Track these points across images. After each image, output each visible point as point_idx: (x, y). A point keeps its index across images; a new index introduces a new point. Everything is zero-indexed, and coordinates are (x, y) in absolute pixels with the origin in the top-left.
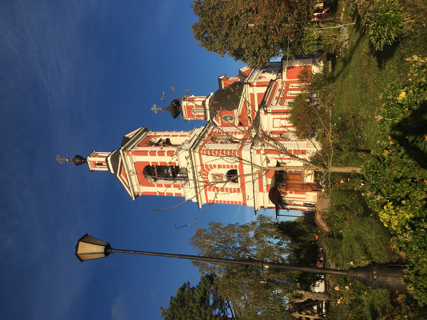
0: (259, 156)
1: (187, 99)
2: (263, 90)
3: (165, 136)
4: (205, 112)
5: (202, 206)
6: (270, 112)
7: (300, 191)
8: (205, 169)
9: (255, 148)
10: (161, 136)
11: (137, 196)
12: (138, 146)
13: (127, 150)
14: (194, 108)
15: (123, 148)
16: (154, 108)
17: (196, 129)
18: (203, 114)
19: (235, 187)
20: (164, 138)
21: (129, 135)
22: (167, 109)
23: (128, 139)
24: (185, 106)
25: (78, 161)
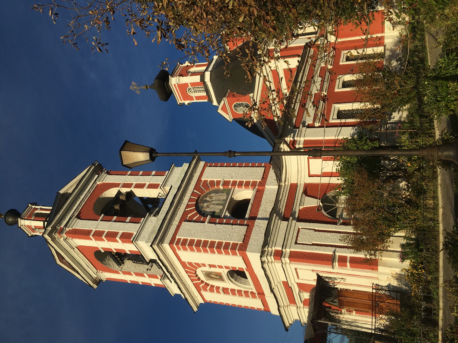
0: (278, 265)
1: (178, 71)
2: (294, 62)
3: (125, 185)
4: (207, 91)
5: (198, 307)
6: (301, 146)
7: (367, 312)
8: (188, 266)
9: (270, 249)
10: (116, 185)
11: (99, 282)
12: (79, 217)
13: (59, 228)
14: (190, 87)
15: (49, 229)
16: (134, 86)
17: (176, 168)
18: (204, 94)
20: (124, 190)
21: (68, 188)
22: (151, 87)
23: (66, 196)
24: (175, 85)
25: (10, 220)
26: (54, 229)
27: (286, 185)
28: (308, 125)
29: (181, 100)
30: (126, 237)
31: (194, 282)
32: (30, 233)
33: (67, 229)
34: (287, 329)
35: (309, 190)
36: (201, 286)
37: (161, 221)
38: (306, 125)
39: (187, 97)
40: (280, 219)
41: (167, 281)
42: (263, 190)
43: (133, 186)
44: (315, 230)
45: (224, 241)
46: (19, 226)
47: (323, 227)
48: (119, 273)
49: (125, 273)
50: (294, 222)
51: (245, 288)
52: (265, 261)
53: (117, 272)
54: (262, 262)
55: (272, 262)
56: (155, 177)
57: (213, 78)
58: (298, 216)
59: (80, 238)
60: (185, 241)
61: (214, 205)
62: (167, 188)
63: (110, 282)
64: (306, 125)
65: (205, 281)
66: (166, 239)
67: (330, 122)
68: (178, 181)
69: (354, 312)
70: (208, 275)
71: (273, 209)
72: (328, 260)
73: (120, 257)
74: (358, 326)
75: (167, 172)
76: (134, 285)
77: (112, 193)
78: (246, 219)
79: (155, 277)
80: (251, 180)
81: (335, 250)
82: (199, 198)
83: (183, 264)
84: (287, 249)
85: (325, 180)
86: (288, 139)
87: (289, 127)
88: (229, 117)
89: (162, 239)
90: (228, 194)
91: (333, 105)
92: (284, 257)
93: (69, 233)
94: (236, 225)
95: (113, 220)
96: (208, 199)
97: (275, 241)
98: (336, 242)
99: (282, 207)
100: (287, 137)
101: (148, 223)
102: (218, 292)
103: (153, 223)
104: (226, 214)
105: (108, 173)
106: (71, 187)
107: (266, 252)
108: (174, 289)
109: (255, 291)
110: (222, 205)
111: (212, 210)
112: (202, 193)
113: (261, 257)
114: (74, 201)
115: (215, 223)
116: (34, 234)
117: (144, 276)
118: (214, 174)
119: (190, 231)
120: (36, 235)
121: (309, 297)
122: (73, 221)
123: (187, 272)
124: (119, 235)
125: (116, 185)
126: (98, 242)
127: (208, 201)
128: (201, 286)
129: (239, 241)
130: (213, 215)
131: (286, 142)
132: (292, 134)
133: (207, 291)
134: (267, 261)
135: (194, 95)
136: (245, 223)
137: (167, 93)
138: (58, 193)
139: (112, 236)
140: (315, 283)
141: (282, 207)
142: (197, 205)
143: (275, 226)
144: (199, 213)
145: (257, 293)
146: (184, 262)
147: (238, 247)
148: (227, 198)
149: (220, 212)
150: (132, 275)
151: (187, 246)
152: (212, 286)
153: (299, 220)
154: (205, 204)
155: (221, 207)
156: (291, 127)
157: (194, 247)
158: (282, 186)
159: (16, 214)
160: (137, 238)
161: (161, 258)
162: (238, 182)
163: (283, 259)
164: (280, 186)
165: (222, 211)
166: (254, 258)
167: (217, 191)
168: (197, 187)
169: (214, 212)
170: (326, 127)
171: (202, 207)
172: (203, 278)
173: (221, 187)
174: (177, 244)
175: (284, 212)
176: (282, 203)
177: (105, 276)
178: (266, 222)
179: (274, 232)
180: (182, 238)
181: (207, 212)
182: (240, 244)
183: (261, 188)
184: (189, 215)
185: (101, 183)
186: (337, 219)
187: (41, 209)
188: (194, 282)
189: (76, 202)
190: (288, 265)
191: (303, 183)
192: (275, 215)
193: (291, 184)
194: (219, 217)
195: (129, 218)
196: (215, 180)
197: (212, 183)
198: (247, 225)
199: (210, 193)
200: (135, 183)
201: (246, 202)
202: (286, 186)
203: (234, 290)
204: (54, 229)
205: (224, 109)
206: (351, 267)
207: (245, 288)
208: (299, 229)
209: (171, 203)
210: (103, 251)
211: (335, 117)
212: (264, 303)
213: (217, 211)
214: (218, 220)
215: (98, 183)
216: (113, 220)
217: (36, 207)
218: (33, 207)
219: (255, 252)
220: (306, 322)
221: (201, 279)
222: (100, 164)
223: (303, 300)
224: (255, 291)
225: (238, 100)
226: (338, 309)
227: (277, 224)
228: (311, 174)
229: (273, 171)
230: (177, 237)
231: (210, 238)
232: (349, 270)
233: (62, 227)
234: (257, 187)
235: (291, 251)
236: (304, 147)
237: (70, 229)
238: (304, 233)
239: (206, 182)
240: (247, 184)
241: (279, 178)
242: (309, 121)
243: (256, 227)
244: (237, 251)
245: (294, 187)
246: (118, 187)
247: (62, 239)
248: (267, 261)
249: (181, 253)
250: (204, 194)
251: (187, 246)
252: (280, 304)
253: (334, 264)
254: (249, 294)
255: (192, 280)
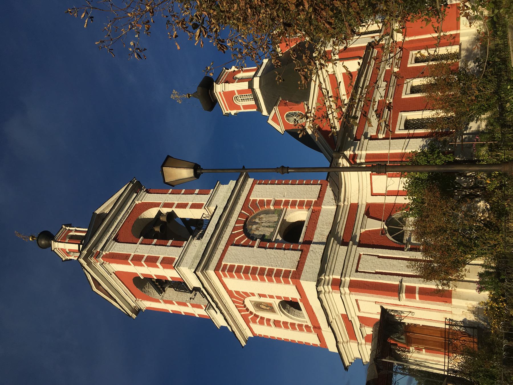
0: (336, 296)
1: (224, 77)
2: (354, 66)
3: (166, 205)
4: (256, 99)
5: (246, 341)
6: (363, 161)
7: (439, 350)
8: (235, 295)
9: (327, 278)
10: (157, 205)
11: (138, 311)
12: (116, 240)
13: (95, 252)
14: (237, 95)
15: (85, 252)
16: (175, 95)
18: (253, 103)
19: (300, 323)
20: (165, 211)
21: (105, 208)
23: (103, 217)
24: (220, 93)
25: (43, 242)
26: (90, 253)
27: (344, 205)
28: (371, 136)
29: (227, 110)
30: (168, 262)
31: (242, 313)
32: (64, 257)
33: (104, 253)
34: (346, 368)
35: (372, 211)
36: (250, 317)
37: (206, 245)
38: (369, 136)
39: (233, 106)
40: (338, 243)
41: (212, 311)
42: (319, 211)
43: (175, 205)
44: (379, 257)
45: (276, 268)
46: (53, 249)
47: (388, 253)
48: (160, 302)
49: (166, 302)
50: (355, 247)
51: (299, 321)
52: (321, 291)
53: (157, 301)
54: (318, 292)
55: (329, 292)
56: (198, 195)
57: (262, 85)
58: (359, 241)
59: (117, 263)
60: (232, 267)
61: (264, 227)
62: (212, 208)
63: (150, 311)
64: (369, 136)
65: (254, 312)
66: (211, 265)
67: (396, 133)
68: (224, 200)
69: (424, 350)
70: (258, 305)
71: (330, 233)
72: (394, 290)
73: (161, 285)
74: (428, 367)
75: (212, 190)
76: (176, 315)
77: (151, 213)
78: (300, 243)
79: (199, 306)
80: (306, 200)
81: (402, 280)
82: (247, 219)
83: (230, 293)
84: (346, 278)
85: (391, 200)
86: (348, 153)
87: (349, 139)
88: (280, 128)
89: (206, 265)
90: (280, 216)
91: (400, 114)
92: (344, 287)
93: (105, 257)
94: (288, 249)
95: (153, 243)
96: (257, 220)
97: (332, 269)
98: (402, 270)
99: (341, 231)
100: (346, 150)
101: (191, 247)
102: (269, 325)
103: (196, 247)
104: (277, 238)
105: (148, 192)
106: (108, 206)
107: (323, 281)
108: (219, 321)
109: (310, 324)
110: (273, 227)
111: (262, 233)
112: (251, 214)
113: (317, 286)
114: (111, 222)
115: (265, 248)
116: (68, 258)
117: (187, 306)
118: (263, 192)
119: (237, 256)
120: (71, 260)
121: (372, 333)
122: (110, 244)
123: (234, 302)
124: (160, 260)
125: (157, 205)
126: (137, 267)
127: (257, 223)
128: (249, 318)
129: (292, 268)
130: (263, 238)
131: (345, 157)
132: (352, 147)
133: (256, 323)
134: (323, 291)
135: (241, 104)
136: (299, 248)
137: (211, 102)
138: (93, 213)
139: (152, 261)
140: (378, 317)
141: (341, 231)
142: (245, 228)
143: (333, 252)
144: (248, 236)
145: (312, 327)
146: (231, 291)
147: (291, 275)
148: (279, 219)
149: (270, 235)
150: (174, 304)
151: (234, 273)
152: (262, 318)
153: (360, 245)
154: (254, 227)
155: (272, 230)
156: (351, 139)
157: (242, 274)
158: (340, 206)
159: (50, 236)
160: (178, 264)
161: (205, 286)
162: (290, 202)
163: (341, 289)
164: (337, 206)
165: (272, 234)
166: (309, 287)
167: (267, 212)
168: (244, 207)
169: (264, 236)
170: (392, 139)
171: (251, 229)
172: (251, 308)
173: (272, 208)
174: (223, 271)
175: (343, 236)
176: (341, 225)
177: (145, 304)
178: (323, 247)
179: (331, 258)
180: (229, 264)
181: (256, 235)
182: (294, 271)
183: (317, 208)
184: (236, 239)
185: (140, 202)
186: (404, 244)
187: (76, 231)
188: (242, 313)
189: (113, 224)
190: (347, 296)
191: (364, 203)
192: (333, 239)
193: (351, 204)
194: (269, 241)
195: (170, 241)
196: (265, 199)
197: (262, 202)
198: (301, 250)
199: (259, 214)
200: (176, 202)
201: (300, 224)
202: (345, 207)
203: (287, 323)
204: (90, 253)
205: (275, 119)
206: (420, 299)
207: (299, 321)
208: (360, 255)
209: (216, 225)
210: (142, 278)
211: (402, 127)
212: (321, 338)
213: (268, 234)
214: (268, 244)
215: (137, 202)
216: (153, 243)
217: (71, 229)
218: (68, 228)
219: (310, 280)
220: (368, 361)
221: (250, 310)
222: (138, 182)
223: (365, 335)
224: (310, 324)
225: (291, 109)
226: (405, 346)
227: (335, 249)
228: (374, 192)
229: (331, 189)
230: (223, 263)
231: (260, 264)
232: (418, 302)
233: (98, 250)
234: (312, 207)
235: (350, 280)
236: (366, 162)
237: (107, 253)
238: (366, 259)
239: (254, 201)
240: (301, 204)
241: (337, 198)
242: (372, 132)
243: (311, 252)
244: (290, 279)
245: (354, 207)
246: (159, 207)
247: (99, 263)
248: (323, 291)
249: (228, 281)
250: (253, 215)
251: (234, 273)
252: (338, 340)
253: (401, 295)
254: (304, 327)
255: (240, 311)
